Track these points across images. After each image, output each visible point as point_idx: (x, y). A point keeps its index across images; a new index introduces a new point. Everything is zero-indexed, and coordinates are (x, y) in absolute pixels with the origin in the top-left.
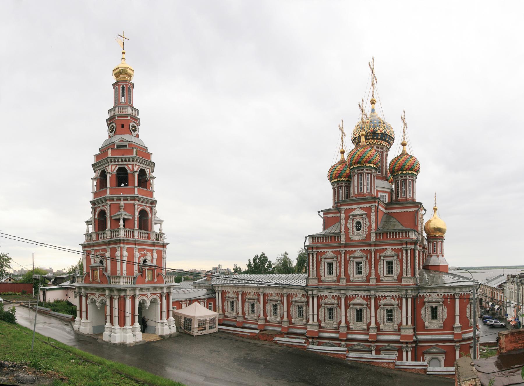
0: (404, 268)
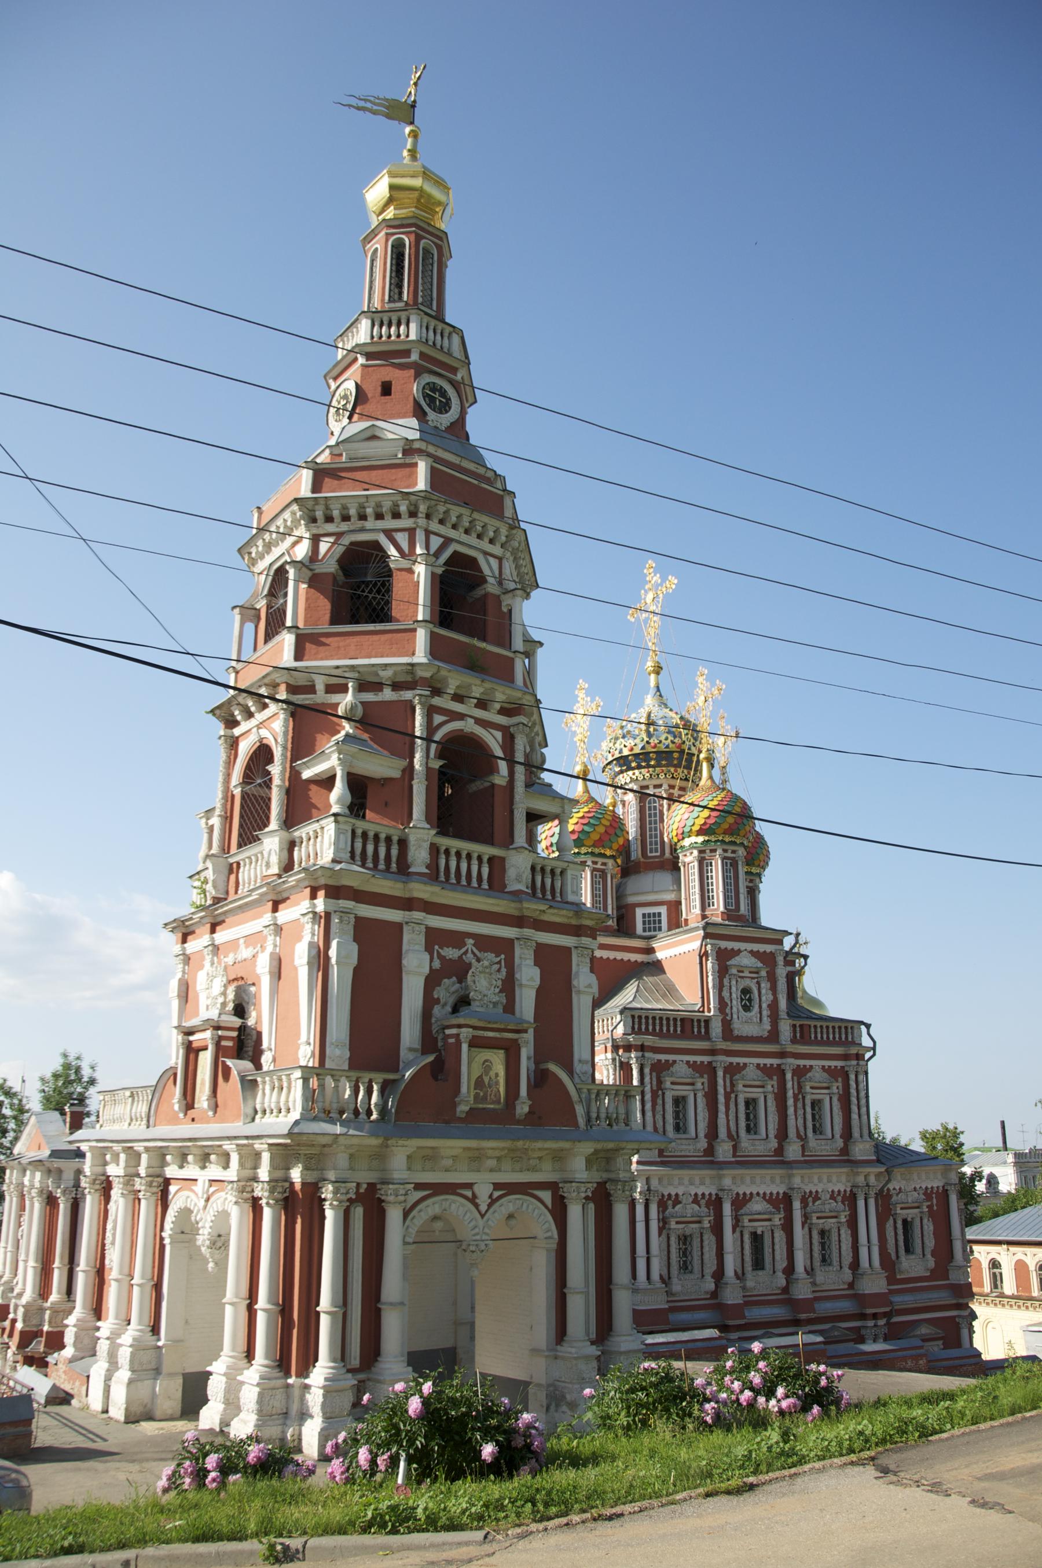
0: (855, 1116)
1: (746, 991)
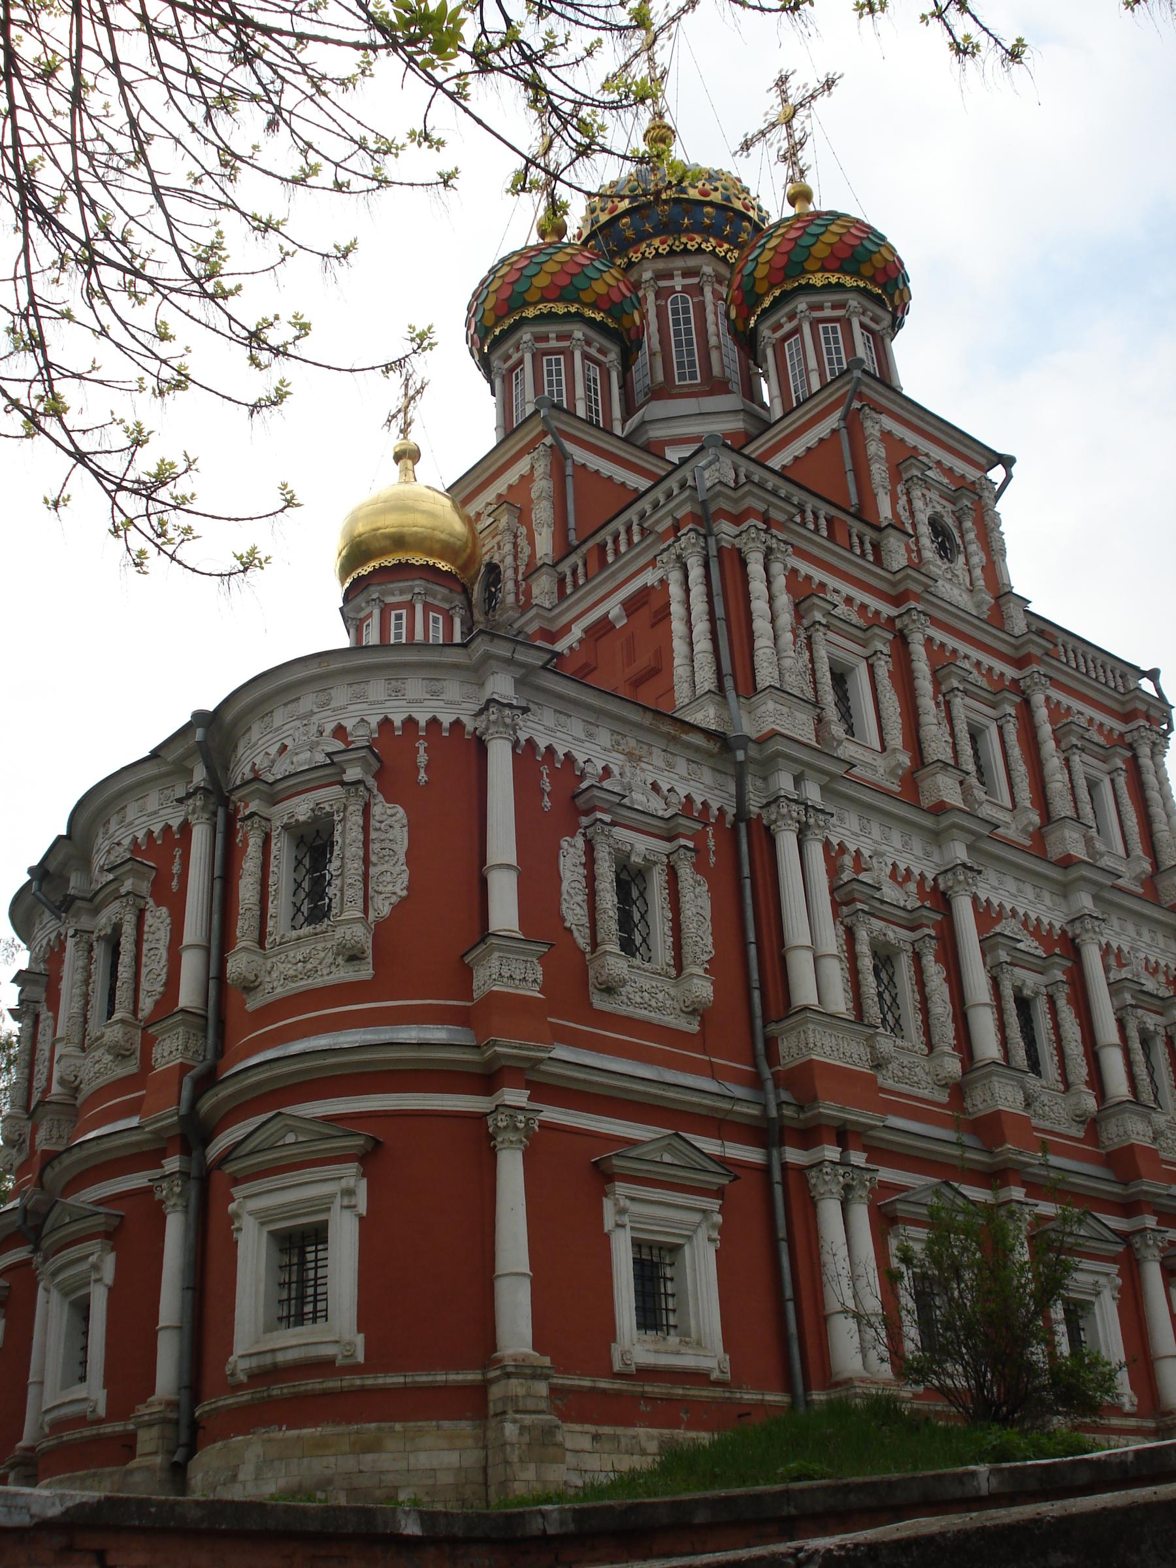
1: (936, 524)
